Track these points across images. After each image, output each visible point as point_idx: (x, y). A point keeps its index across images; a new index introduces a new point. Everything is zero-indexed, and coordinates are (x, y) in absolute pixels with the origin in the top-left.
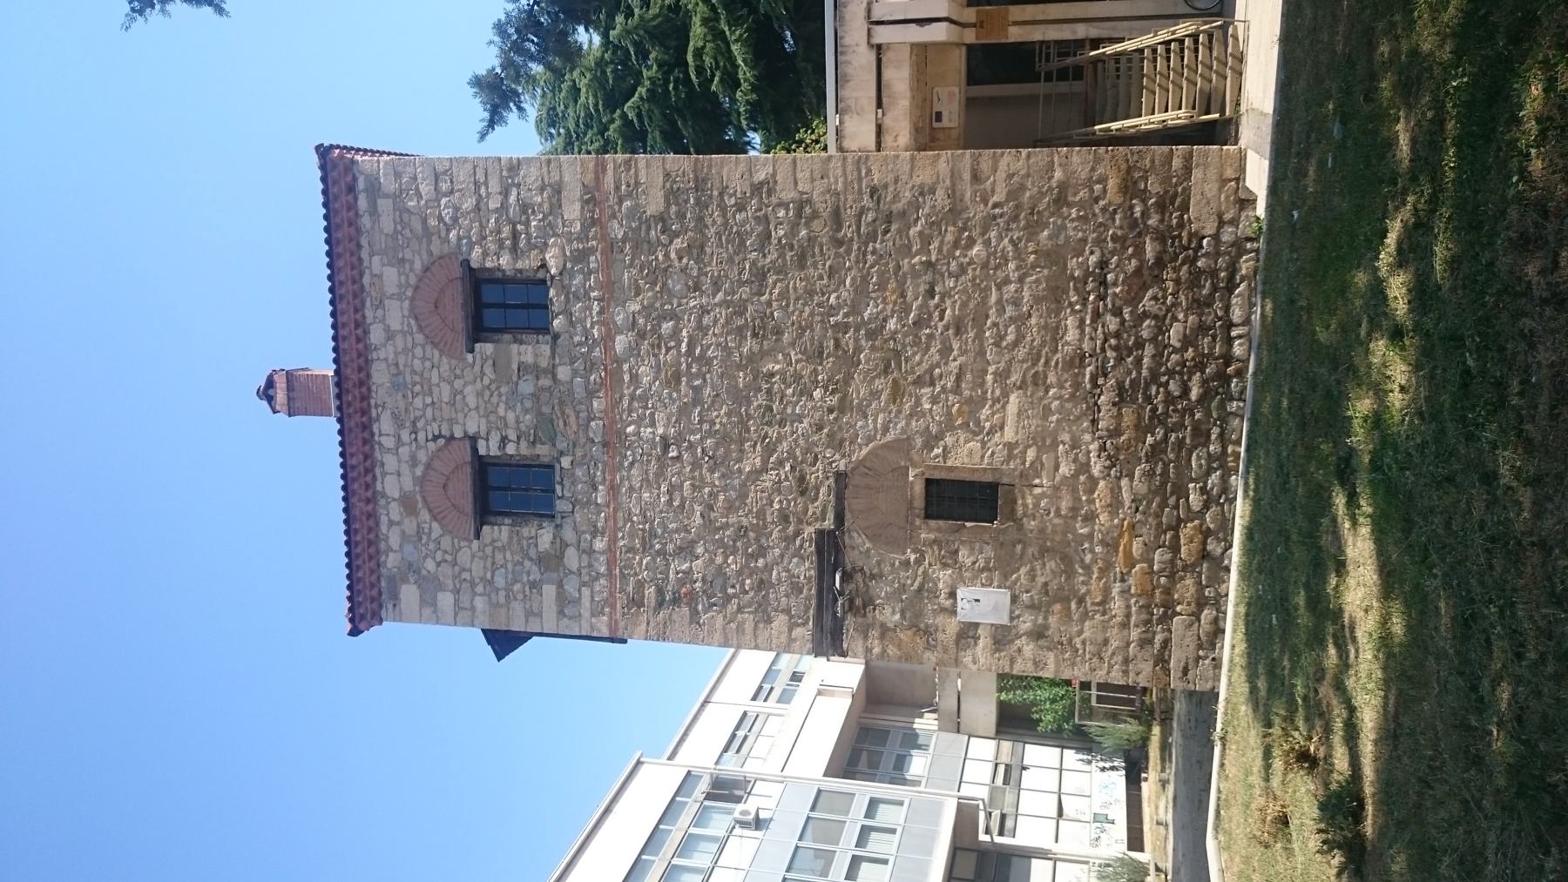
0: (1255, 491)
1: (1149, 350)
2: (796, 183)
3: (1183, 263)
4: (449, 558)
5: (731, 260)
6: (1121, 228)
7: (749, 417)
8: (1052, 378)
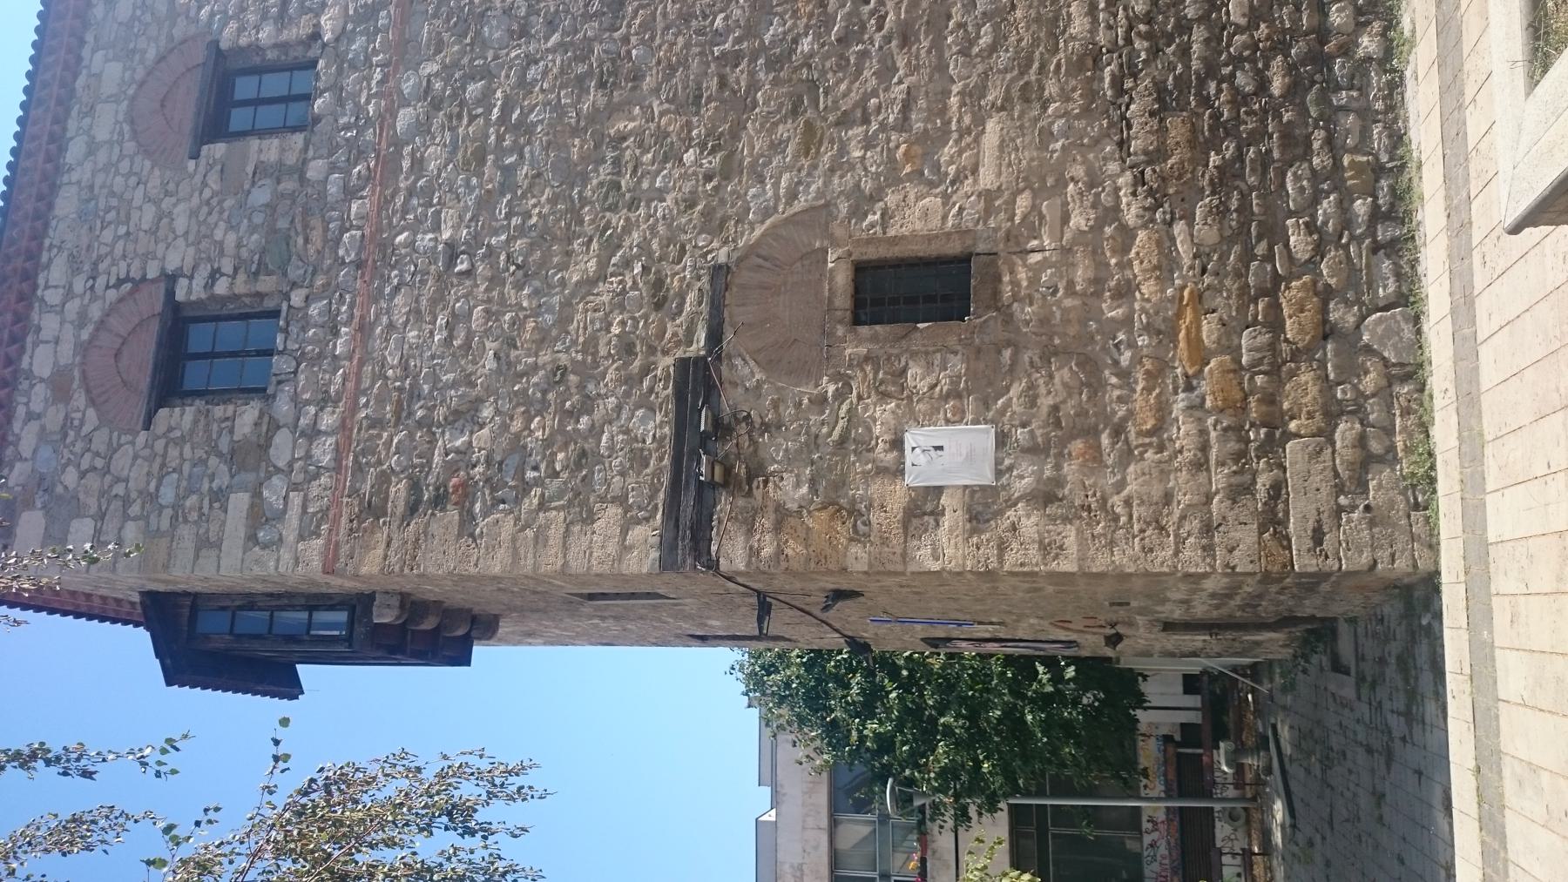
1: (1198, 34)
4: (99, 463)
7: (584, 201)
8: (1051, 88)
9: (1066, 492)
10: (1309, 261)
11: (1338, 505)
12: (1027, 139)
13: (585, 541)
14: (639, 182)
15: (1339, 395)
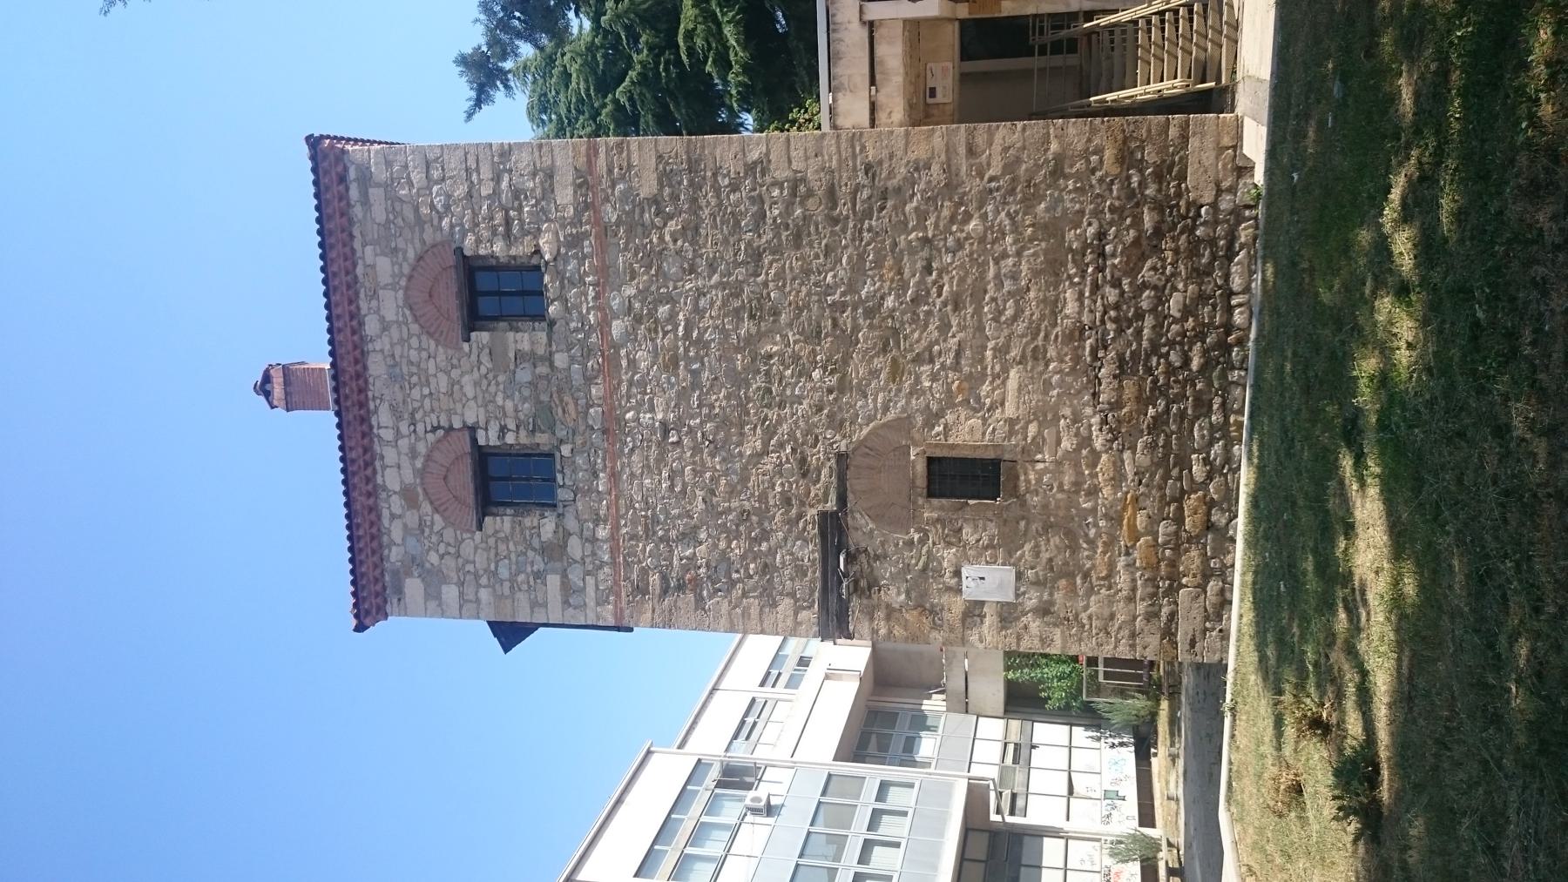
0: (1259, 458)
1: (1149, 321)
2: (790, 162)
3: (1182, 233)
4: (452, 550)
5: (726, 241)
6: (1118, 198)
8: (1052, 352)
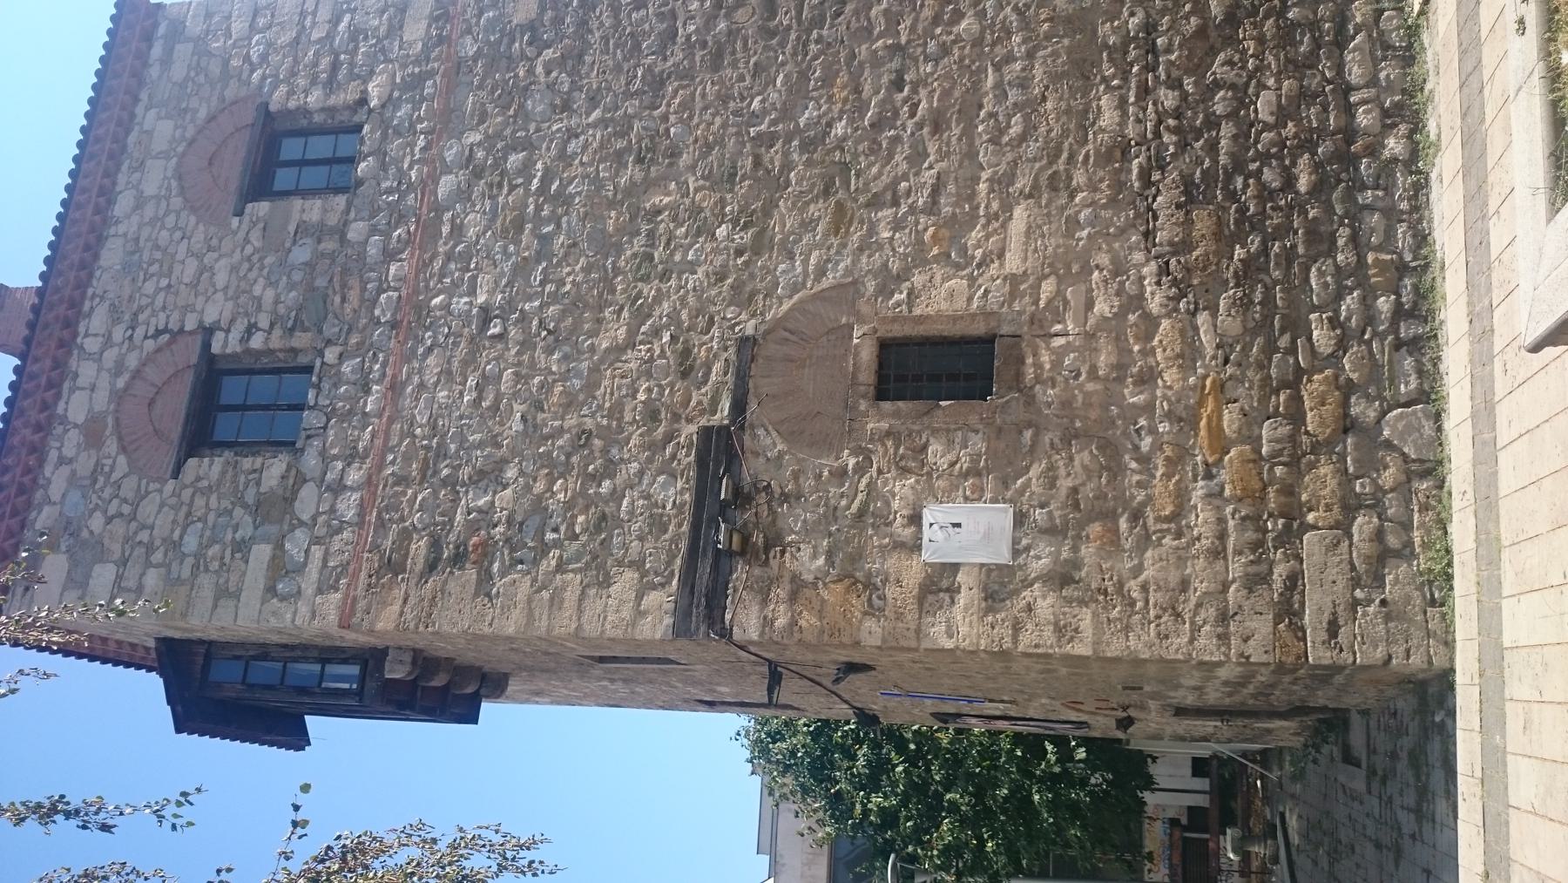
1: (1227, 130)
3: (1266, 17)
4: (126, 509)
5: (618, 69)
7: (617, 271)
8: (1079, 178)
9: (1083, 574)
10: (1332, 355)
11: (1354, 598)
12: (1054, 227)
13: (599, 604)
14: (672, 254)
15: (1358, 489)
